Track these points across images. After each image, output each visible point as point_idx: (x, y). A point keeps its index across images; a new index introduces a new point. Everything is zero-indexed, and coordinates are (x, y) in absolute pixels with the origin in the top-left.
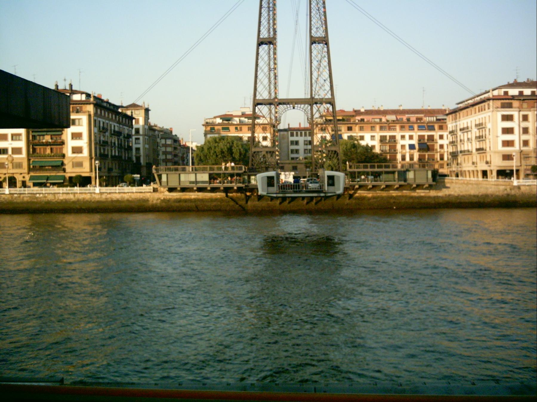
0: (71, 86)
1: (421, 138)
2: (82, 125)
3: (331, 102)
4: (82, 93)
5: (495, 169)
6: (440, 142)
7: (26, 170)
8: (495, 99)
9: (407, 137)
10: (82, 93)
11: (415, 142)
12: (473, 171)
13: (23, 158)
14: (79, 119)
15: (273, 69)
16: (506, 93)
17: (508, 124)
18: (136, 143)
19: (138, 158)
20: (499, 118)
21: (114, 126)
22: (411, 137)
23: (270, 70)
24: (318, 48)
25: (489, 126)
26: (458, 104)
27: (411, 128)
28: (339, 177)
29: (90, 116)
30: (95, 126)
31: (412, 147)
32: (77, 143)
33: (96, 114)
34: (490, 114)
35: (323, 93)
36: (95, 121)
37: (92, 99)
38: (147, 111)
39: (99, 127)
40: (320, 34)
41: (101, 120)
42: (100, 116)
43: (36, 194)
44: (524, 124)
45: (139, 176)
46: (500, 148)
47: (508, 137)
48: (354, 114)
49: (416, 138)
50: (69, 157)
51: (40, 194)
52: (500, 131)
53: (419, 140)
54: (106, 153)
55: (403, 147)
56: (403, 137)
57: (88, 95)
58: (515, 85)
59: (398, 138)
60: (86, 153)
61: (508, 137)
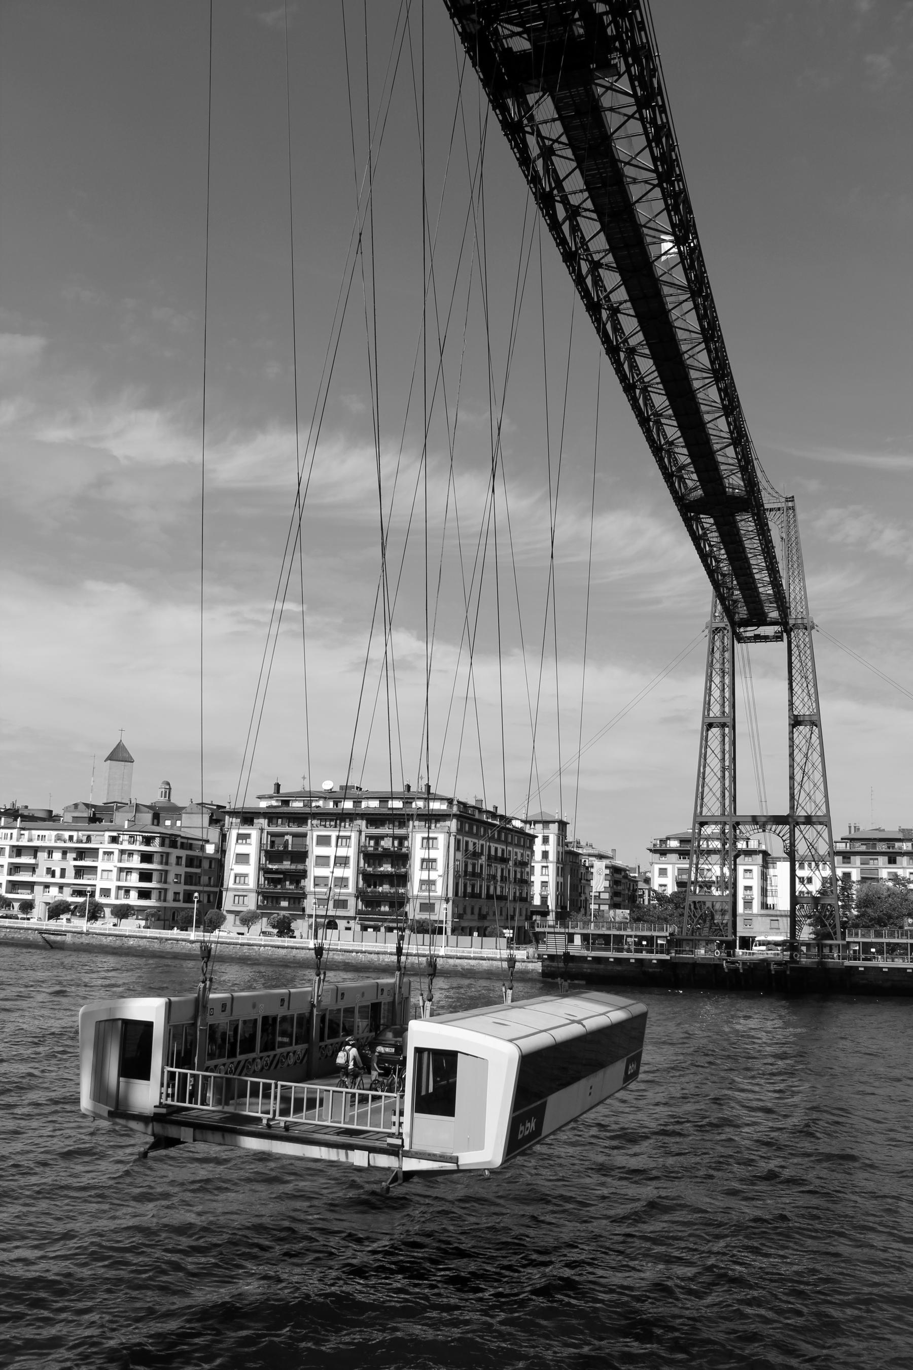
3: (825, 821)
4: (442, 799)
7: (351, 912)
13: (349, 895)
18: (542, 875)
19: (544, 899)
21: (496, 849)
23: (723, 769)
30: (457, 848)
33: (460, 831)
37: (455, 809)
38: (563, 825)
39: (467, 850)
41: (469, 839)
42: (470, 833)
48: (900, 836)
54: (477, 890)
57: (450, 801)
60: (439, 890)
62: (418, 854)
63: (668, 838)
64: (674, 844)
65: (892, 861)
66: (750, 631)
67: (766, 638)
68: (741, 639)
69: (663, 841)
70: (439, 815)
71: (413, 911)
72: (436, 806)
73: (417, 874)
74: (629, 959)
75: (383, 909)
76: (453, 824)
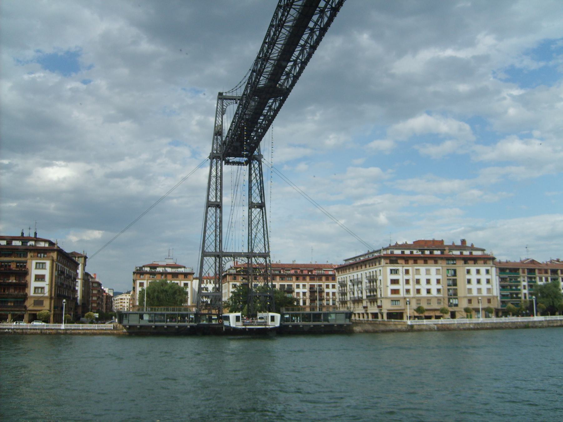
0: (36, 234)
1: (312, 287)
2: (45, 269)
4: (45, 241)
5: (385, 311)
6: (326, 290)
8: (385, 257)
9: (301, 286)
10: (45, 241)
11: (307, 290)
12: (363, 314)
14: (43, 263)
15: (219, 227)
16: (392, 253)
17: (395, 277)
20: (389, 271)
22: (304, 286)
24: (256, 212)
25: (379, 278)
26: (346, 260)
27: (304, 279)
28: (277, 316)
29: (53, 261)
31: (304, 294)
32: (40, 284)
34: (381, 268)
35: (259, 248)
36: (56, 265)
38: (86, 258)
40: (256, 199)
43: (5, 329)
44: (406, 277)
45: (98, 314)
46: (389, 294)
47: (395, 287)
49: (308, 286)
50: (32, 297)
51: (8, 329)
52: (389, 282)
53: (310, 288)
55: (298, 294)
56: (298, 286)
57: (51, 243)
58: (397, 247)
59: (294, 286)
60: (47, 293)
61: (395, 287)
62: (34, 272)
63: (144, 266)
64: (148, 269)
65: (255, 279)
66: (232, 159)
67: (239, 163)
68: (228, 163)
69: (141, 268)
70: (40, 250)
71: (29, 304)
72: (42, 244)
73: (33, 284)
74: (175, 326)
75: (9, 304)
76: (54, 255)
